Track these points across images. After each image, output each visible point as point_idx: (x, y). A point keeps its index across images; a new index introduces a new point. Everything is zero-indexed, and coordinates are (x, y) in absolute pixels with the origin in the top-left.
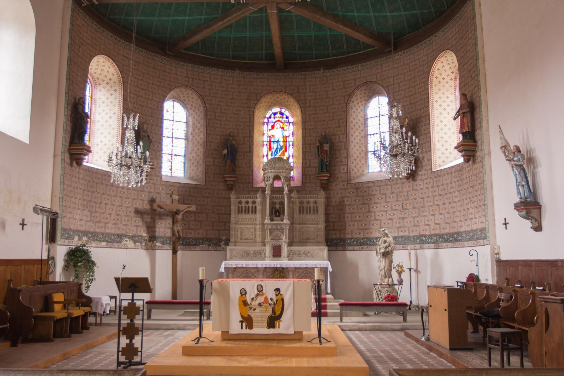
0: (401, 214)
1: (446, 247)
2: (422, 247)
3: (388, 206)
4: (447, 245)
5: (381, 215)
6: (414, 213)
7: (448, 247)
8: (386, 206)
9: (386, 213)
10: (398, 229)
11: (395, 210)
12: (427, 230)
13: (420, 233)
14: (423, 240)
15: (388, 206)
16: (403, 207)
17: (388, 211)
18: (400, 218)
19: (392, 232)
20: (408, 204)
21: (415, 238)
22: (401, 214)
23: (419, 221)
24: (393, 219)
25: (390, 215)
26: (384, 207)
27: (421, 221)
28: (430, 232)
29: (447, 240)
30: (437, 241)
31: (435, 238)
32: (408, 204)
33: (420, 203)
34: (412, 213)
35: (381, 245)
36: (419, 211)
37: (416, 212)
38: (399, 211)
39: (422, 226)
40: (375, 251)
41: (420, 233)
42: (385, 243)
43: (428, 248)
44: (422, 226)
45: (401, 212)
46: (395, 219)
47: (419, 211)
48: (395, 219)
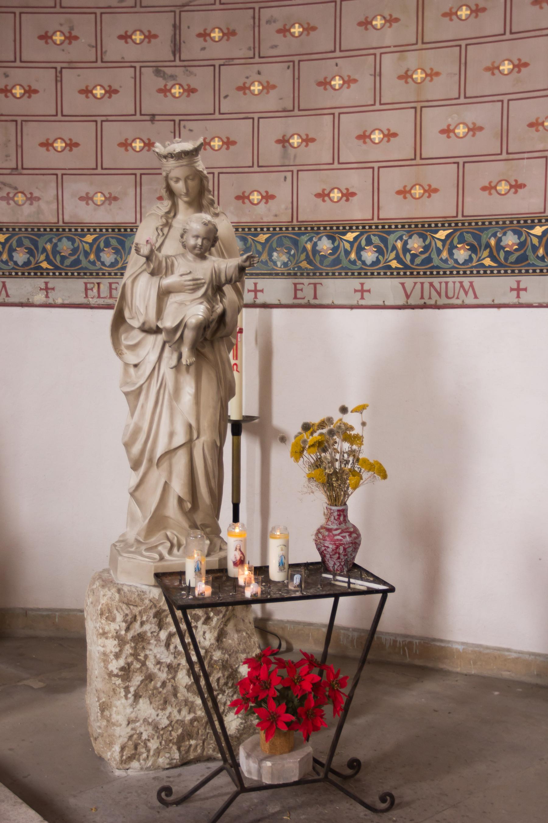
0: (165, 91)
1: (512, 298)
2: (307, 293)
3: (71, 38)
4: (518, 290)
5: (18, 91)
6: (256, 88)
7: (525, 298)
8: (58, 38)
9: (59, 79)
10: (138, 184)
11: (121, 64)
12: (348, 195)
13: (294, 207)
14: (315, 251)
15: (71, 38)
16: (176, 49)
17: (71, 65)
18: (153, 118)
19: (99, 198)
20: (216, 35)
21: (262, 238)
22: (165, 91)
23: (295, 141)
24: (107, 118)
25: (87, 92)
26: (46, 37)
27: (308, 140)
28: (376, 206)
29: (522, 259)
30: (429, 260)
31: (415, 244)
32: (216, 35)
33: (309, 29)
34: (244, 88)
35: (169, 270)
36: (296, 80)
37: (268, 87)
38: (148, 72)
39: (316, 168)
40: (110, 314)
41: (294, 207)
42: (202, 256)
43: (355, 299)
44: (316, 168)
45: (161, 83)
46: (123, 118)
47: (296, 80)
48: (123, 118)
